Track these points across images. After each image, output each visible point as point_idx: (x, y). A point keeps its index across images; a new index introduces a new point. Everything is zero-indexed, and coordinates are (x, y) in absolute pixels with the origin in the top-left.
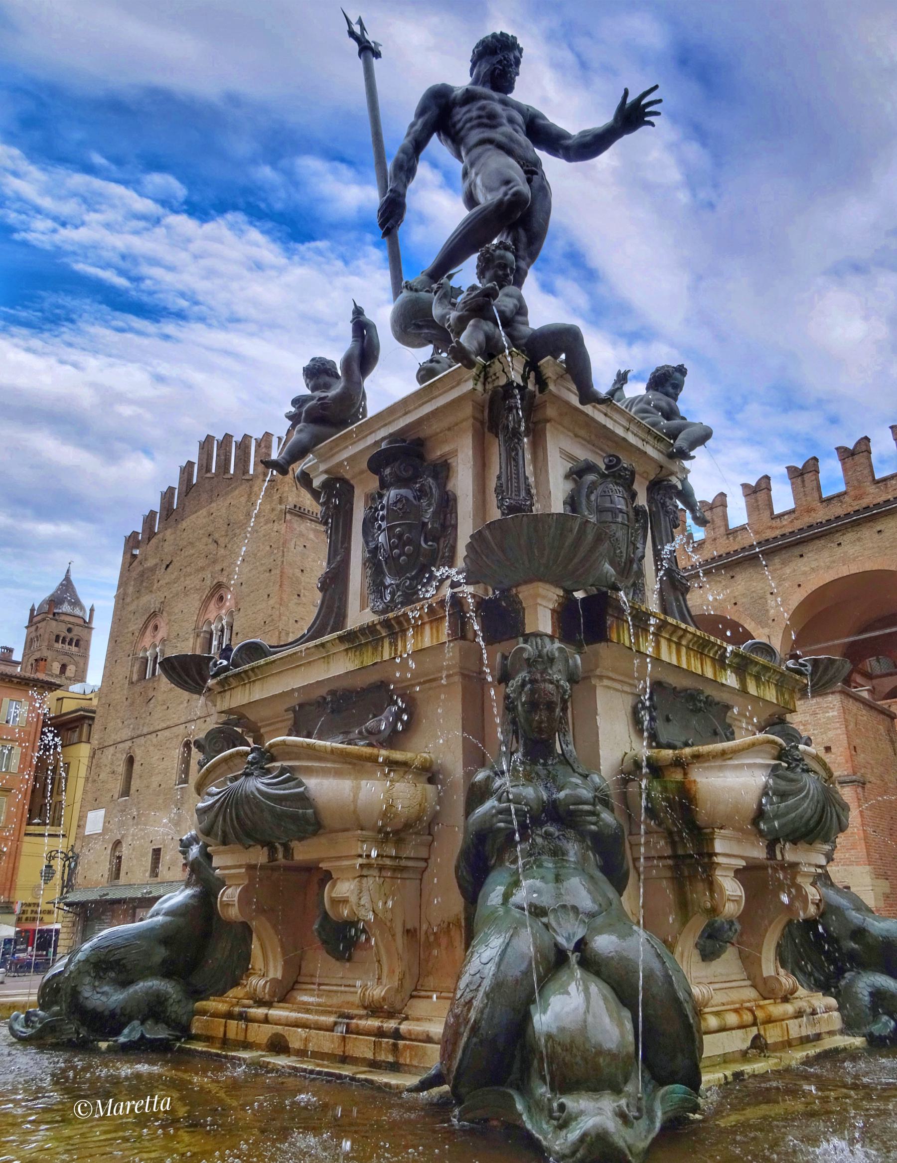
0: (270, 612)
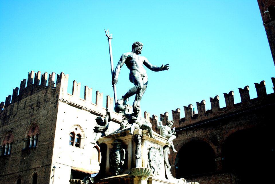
0: (51, 135)
